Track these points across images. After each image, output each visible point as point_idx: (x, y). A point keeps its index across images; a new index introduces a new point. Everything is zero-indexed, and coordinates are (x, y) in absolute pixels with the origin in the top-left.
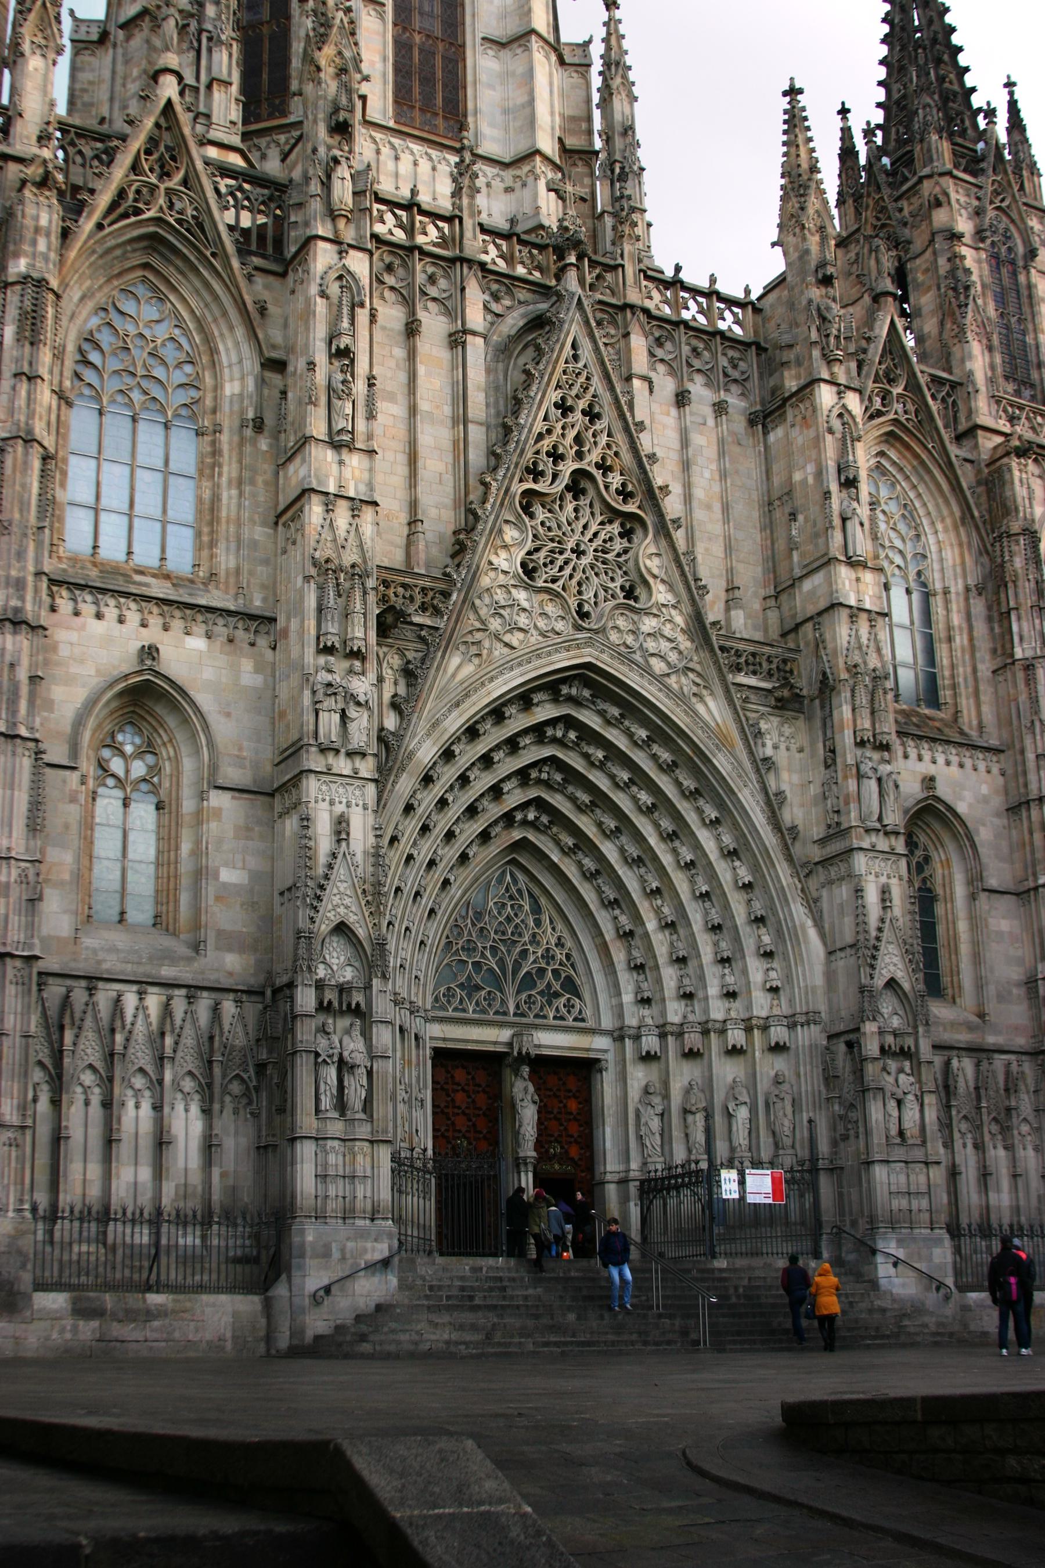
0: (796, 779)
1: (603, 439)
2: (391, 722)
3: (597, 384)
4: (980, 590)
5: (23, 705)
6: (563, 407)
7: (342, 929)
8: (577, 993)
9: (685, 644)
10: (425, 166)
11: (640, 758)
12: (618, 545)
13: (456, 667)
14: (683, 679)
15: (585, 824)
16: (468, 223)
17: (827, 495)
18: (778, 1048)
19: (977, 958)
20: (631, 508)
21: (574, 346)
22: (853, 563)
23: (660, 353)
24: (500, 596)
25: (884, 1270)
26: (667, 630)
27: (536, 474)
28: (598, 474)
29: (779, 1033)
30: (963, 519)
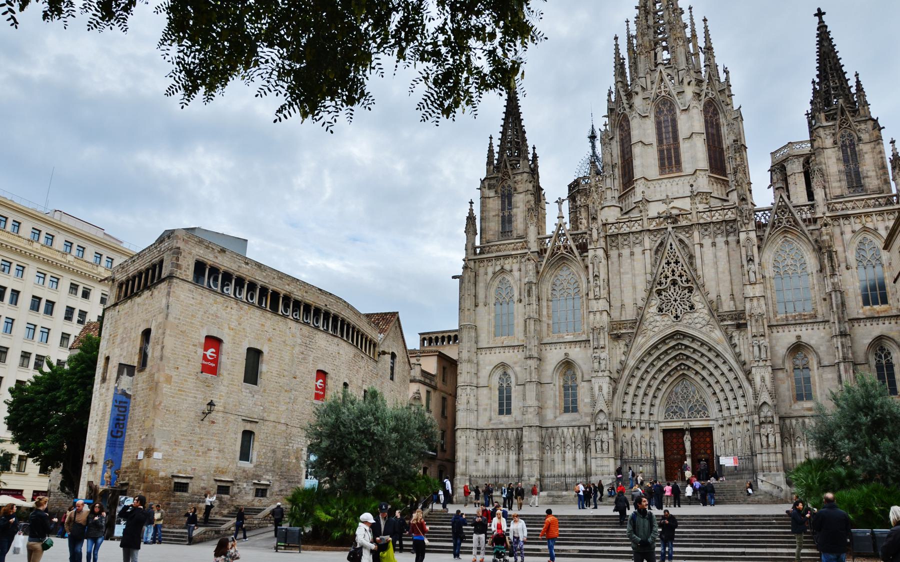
0: (746, 347)
1: (680, 268)
2: (623, 358)
3: (678, 253)
4: (821, 271)
5: (533, 375)
6: (668, 263)
7: (601, 411)
8: (707, 410)
9: (707, 318)
10: (669, 185)
11: (701, 349)
12: (688, 295)
13: (640, 340)
14: (708, 327)
15: (697, 368)
16: (645, 219)
17: (742, 266)
18: (747, 422)
19: (820, 387)
20: (690, 285)
21: (671, 245)
22: (751, 284)
23: (707, 233)
24: (652, 319)
25: (759, 483)
26: (702, 315)
27: (660, 284)
28: (679, 279)
29: (745, 418)
30: (814, 250)
